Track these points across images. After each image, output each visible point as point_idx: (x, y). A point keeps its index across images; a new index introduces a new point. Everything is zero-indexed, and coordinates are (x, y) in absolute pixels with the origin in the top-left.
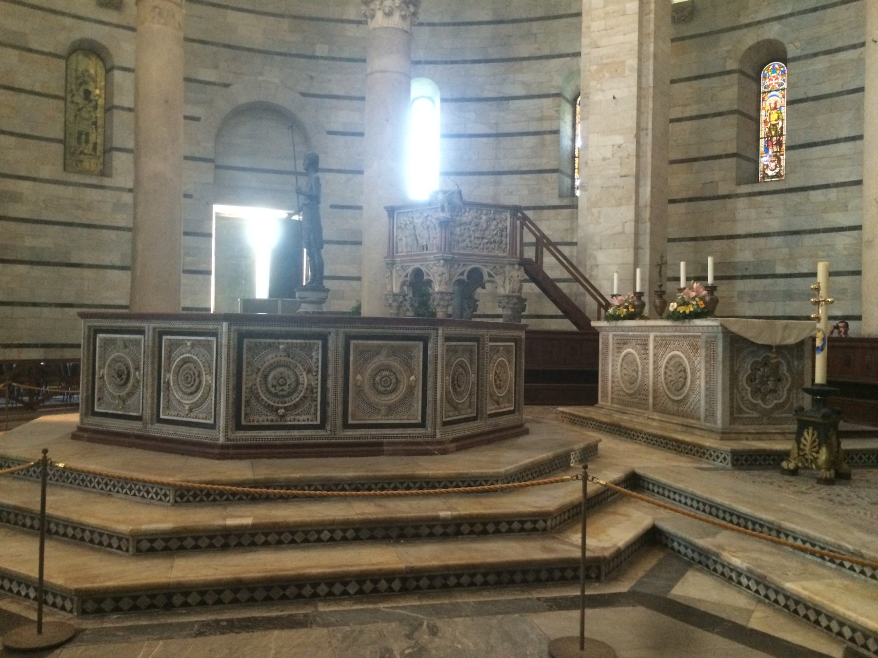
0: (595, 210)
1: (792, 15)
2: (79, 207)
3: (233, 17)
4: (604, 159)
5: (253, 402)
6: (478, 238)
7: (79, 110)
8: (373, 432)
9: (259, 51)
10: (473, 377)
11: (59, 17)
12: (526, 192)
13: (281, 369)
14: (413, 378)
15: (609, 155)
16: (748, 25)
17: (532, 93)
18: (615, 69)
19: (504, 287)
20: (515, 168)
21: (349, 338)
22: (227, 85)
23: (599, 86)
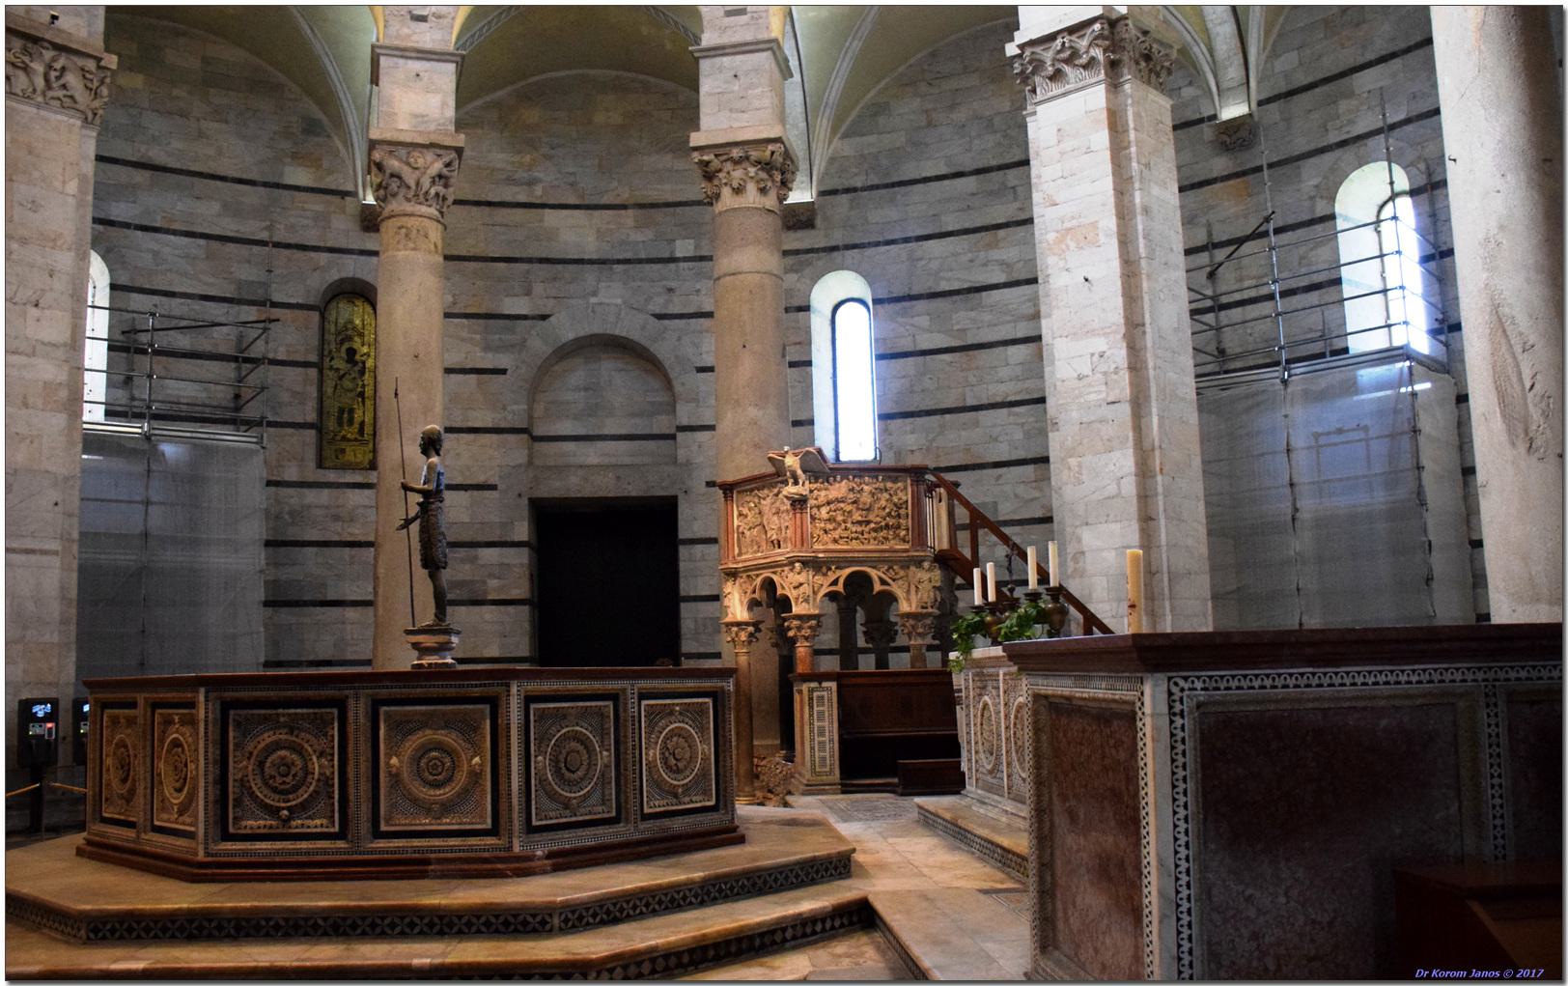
0: (1073, 462)
1: (1408, 121)
2: (337, 518)
3: (551, 217)
4: (1080, 378)
5: (247, 801)
6: (860, 523)
7: (341, 378)
8: (416, 842)
9: (591, 262)
10: (605, 757)
11: (313, 254)
12: (1019, 435)
13: (283, 753)
14: (477, 760)
15: (1087, 371)
16: (1343, 144)
17: (1016, 276)
18: (1086, 236)
19: (908, 600)
20: (999, 399)
21: (376, 704)
22: (544, 317)
23: (1061, 264)
